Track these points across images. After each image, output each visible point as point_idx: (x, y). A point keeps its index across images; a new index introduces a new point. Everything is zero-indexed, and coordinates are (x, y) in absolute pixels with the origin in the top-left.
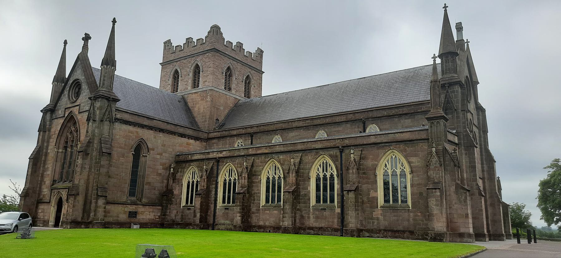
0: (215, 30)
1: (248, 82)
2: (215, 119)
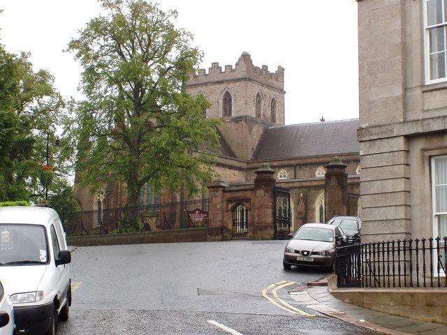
0: (246, 58)
1: (273, 103)
2: (250, 149)
